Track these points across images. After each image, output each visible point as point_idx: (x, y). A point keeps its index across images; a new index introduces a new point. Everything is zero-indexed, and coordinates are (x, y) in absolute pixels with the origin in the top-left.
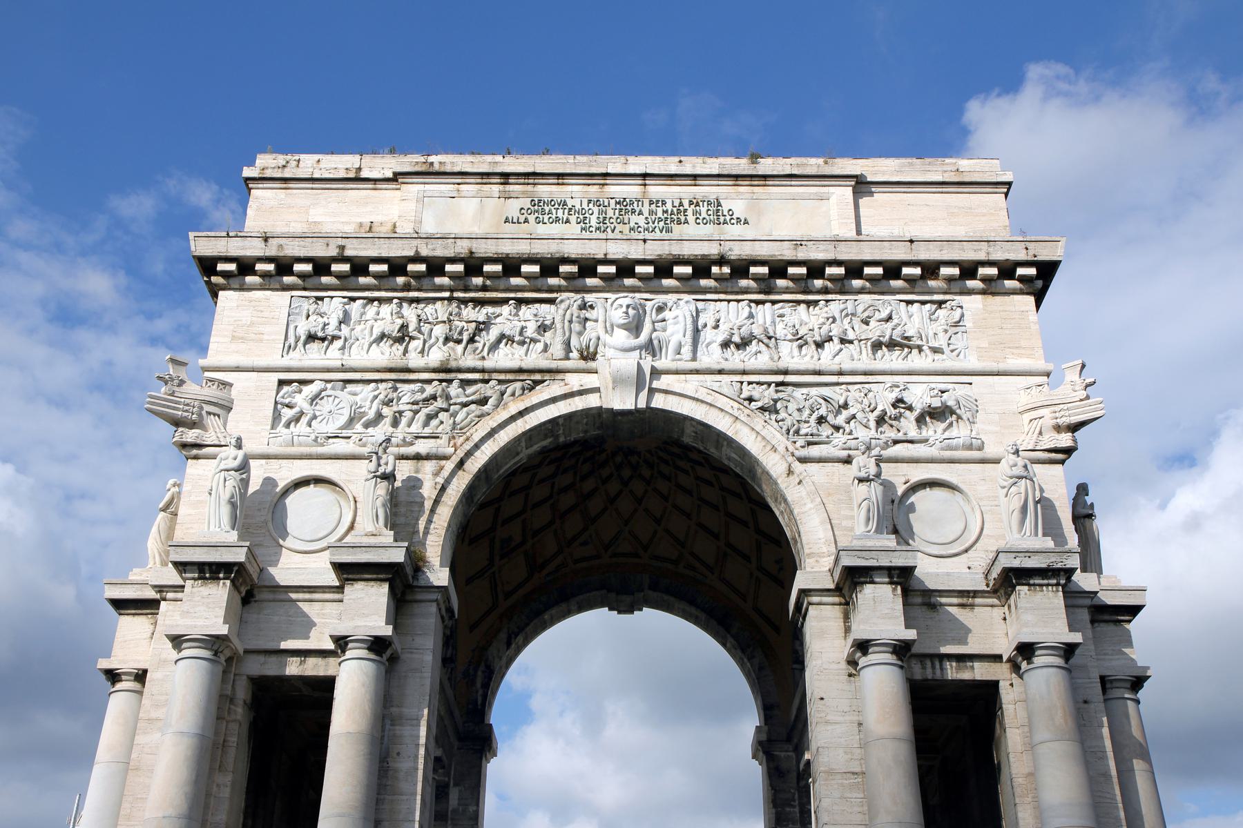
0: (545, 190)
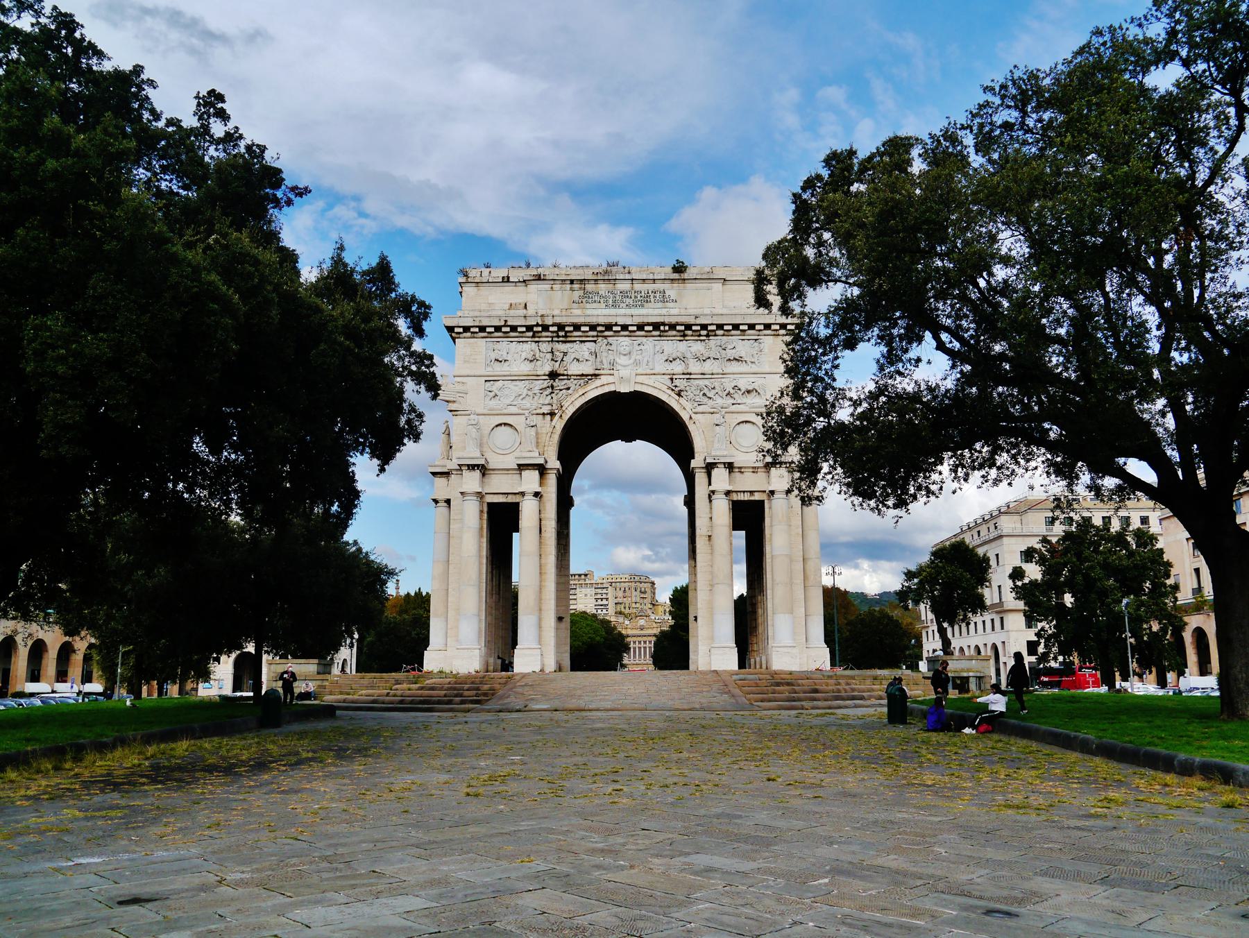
0: (589, 287)
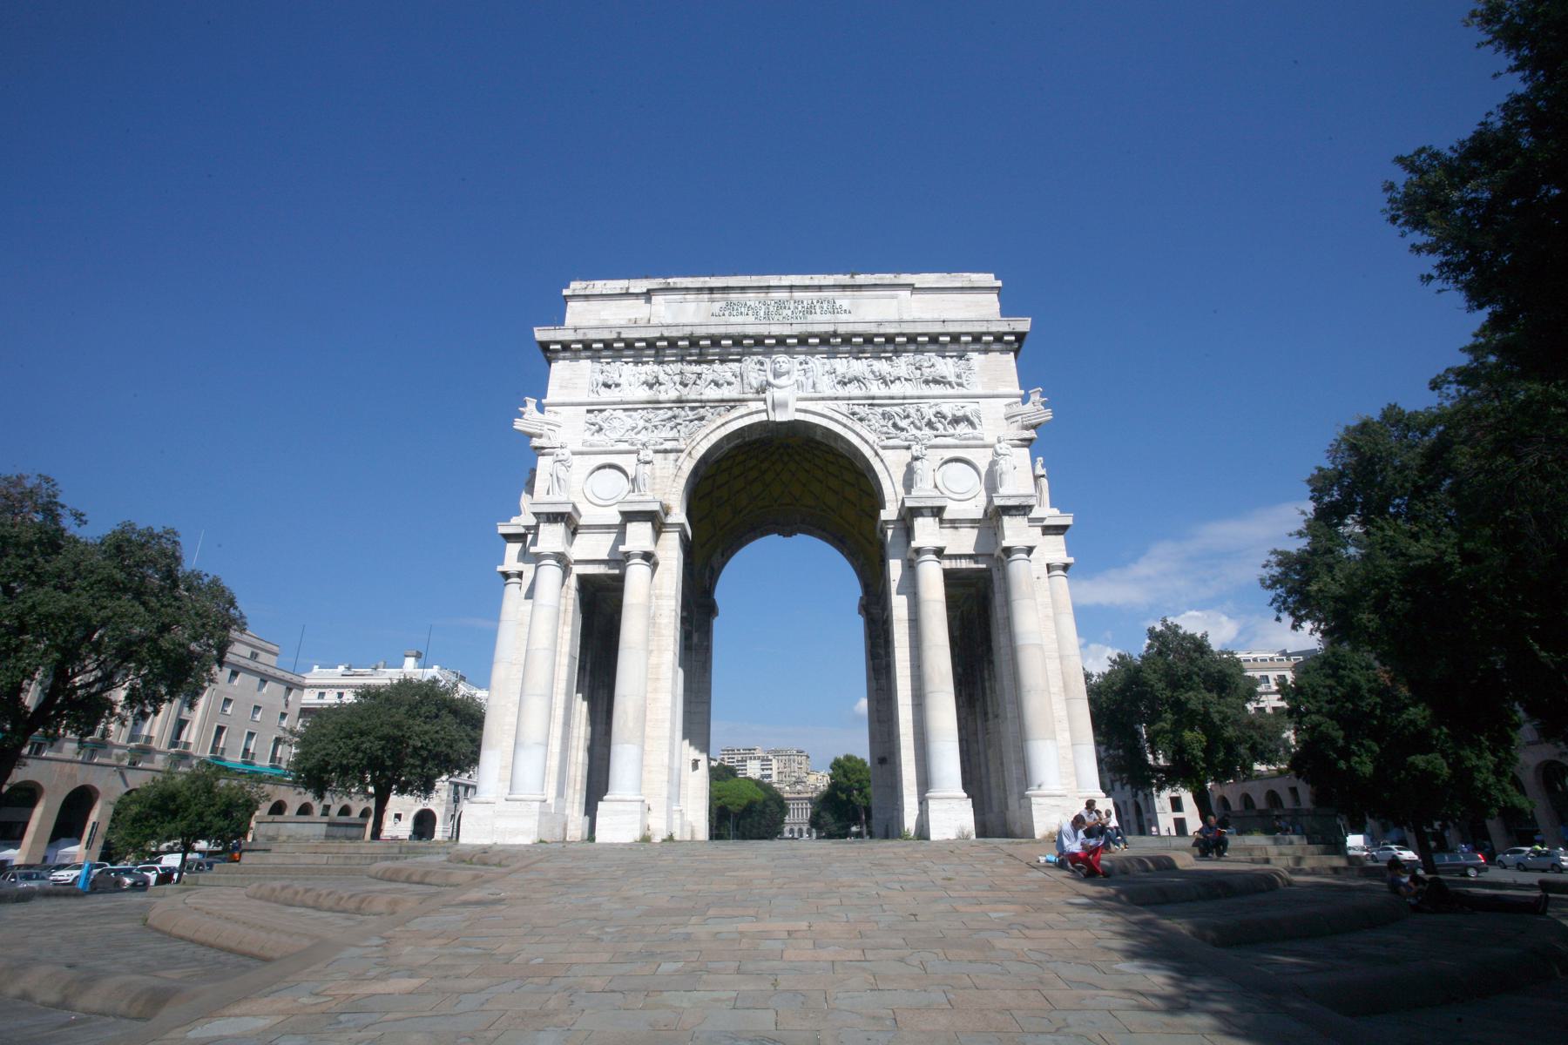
0: (733, 296)
